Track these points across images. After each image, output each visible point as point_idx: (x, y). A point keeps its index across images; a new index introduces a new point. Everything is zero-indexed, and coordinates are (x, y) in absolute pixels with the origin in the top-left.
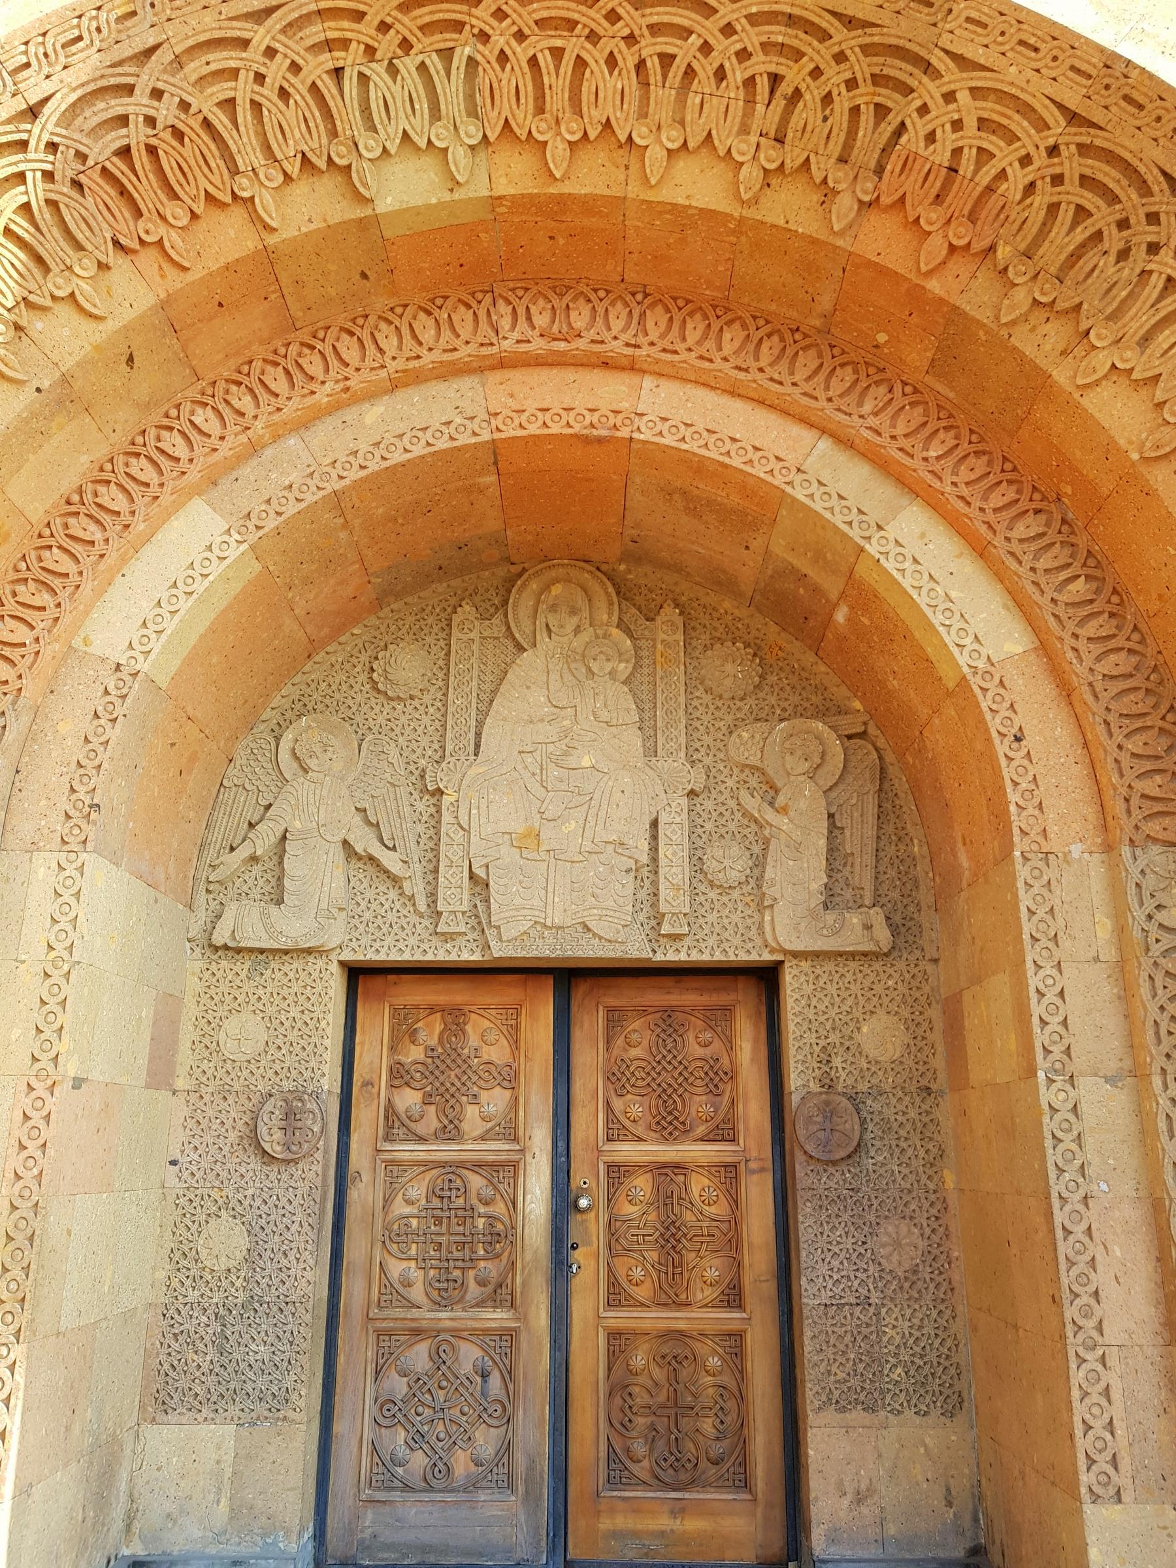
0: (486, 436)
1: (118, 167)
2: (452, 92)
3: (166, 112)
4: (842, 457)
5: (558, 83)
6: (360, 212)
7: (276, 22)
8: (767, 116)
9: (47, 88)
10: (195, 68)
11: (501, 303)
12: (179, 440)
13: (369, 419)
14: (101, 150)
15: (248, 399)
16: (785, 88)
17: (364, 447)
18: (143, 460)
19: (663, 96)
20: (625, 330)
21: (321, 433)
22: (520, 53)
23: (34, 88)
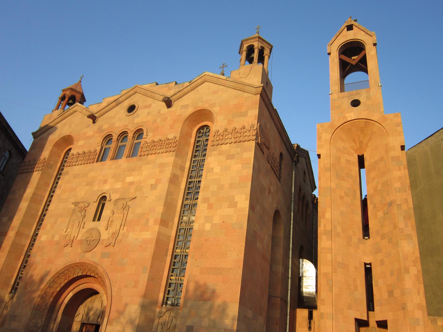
21: (78, 287)
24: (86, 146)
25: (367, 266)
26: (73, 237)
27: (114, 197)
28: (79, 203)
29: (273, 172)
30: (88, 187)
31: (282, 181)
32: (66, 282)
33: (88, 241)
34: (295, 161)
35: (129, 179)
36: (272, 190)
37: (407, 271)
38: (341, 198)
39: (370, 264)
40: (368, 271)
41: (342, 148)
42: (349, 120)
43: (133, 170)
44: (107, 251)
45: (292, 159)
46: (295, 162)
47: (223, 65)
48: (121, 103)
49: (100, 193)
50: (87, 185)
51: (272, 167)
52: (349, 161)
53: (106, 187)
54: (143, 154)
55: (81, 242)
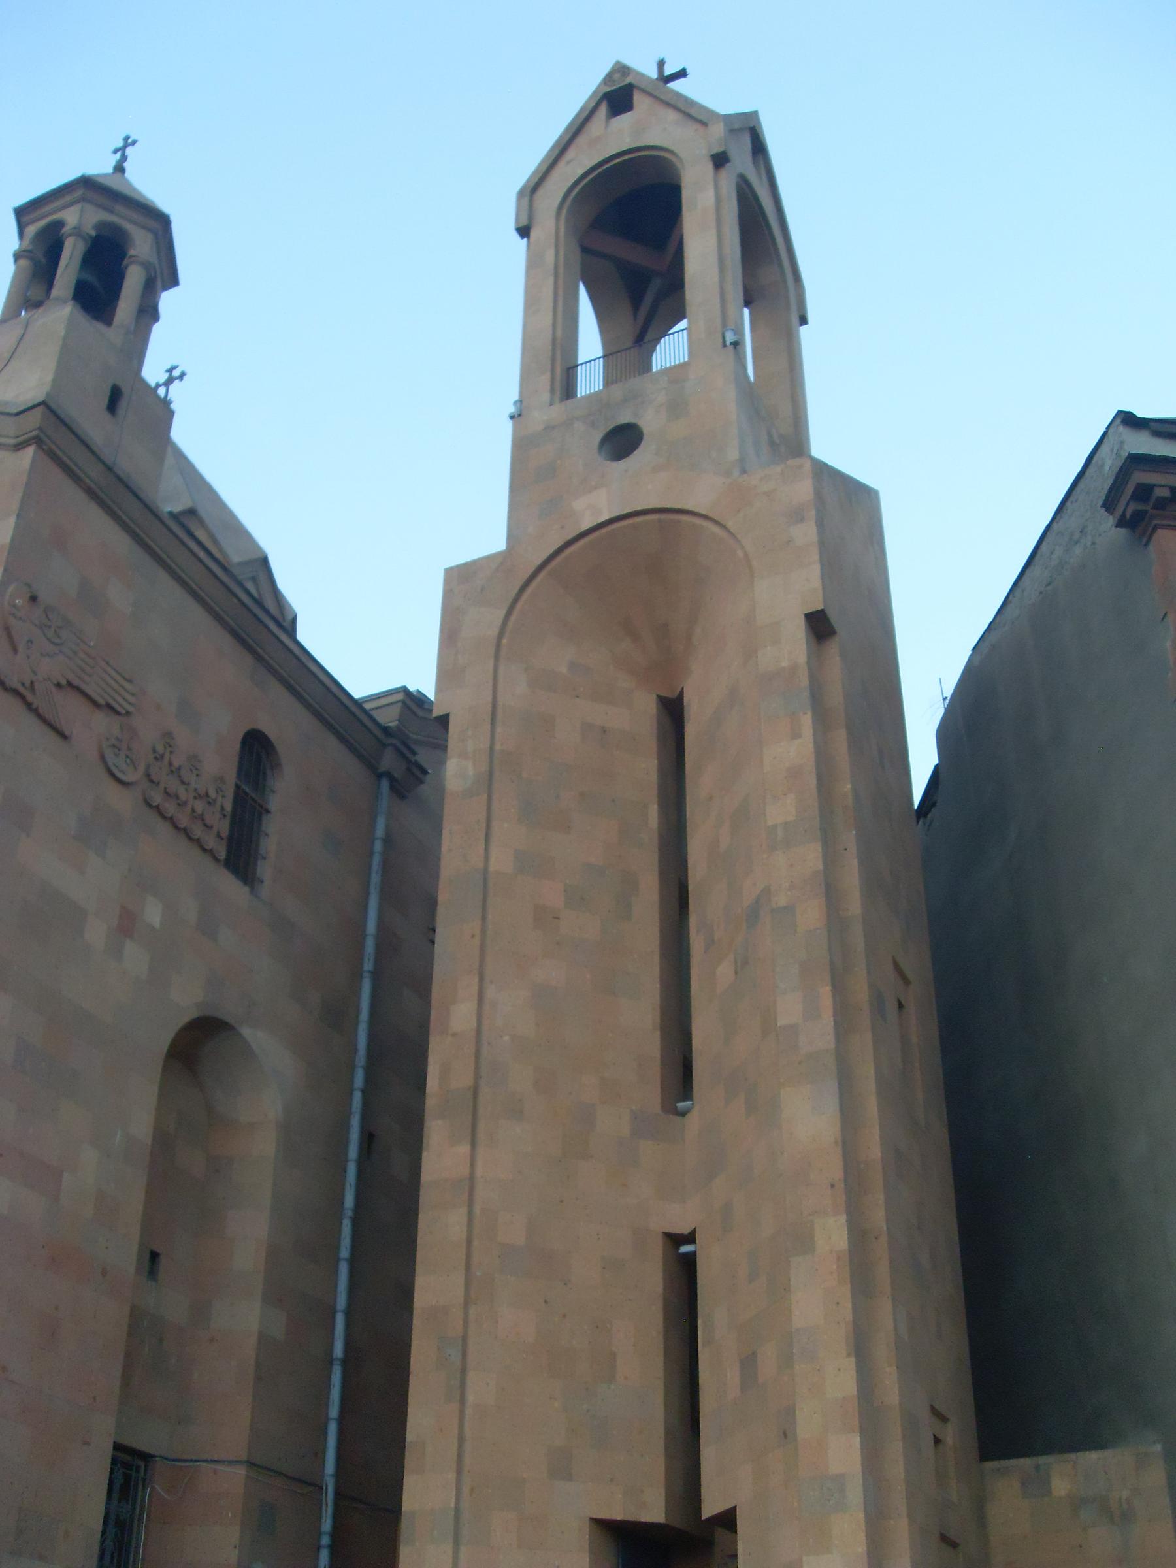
25: (685, 1249)
29: (163, 828)
31: (265, 870)
34: (388, 775)
36: (153, 914)
37: (803, 1241)
38: (544, 917)
39: (691, 1238)
40: (683, 1271)
41: (564, 670)
42: (586, 524)
45: (370, 764)
46: (392, 780)
47: (170, 371)
51: (148, 804)
52: (604, 731)
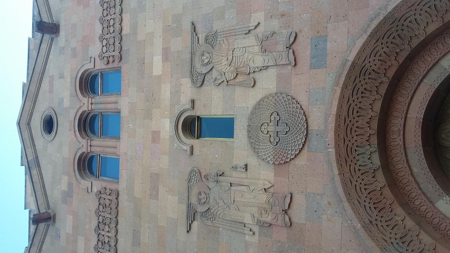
0: (422, 148)
1: (378, 210)
2: (361, 150)
3: (368, 200)
4: (428, 77)
5: (359, 131)
6: (381, 168)
7: (352, 180)
8: (368, 94)
9: (367, 219)
10: (360, 194)
11: (391, 144)
12: (422, 208)
13: (417, 171)
14: (376, 212)
15: (413, 194)
16: (364, 91)
17: (423, 172)
18: (427, 215)
19: (363, 113)
20: (398, 120)
21: (419, 180)
22: (355, 138)
23: (367, 221)
24: (87, 226)
26: (264, 197)
27: (187, 90)
28: (189, 205)
30: (162, 190)
32: (399, 210)
33: (279, 129)
35: (157, 66)
43: (142, 62)
44: (308, 52)
48: (37, 157)
49: (177, 143)
50: (156, 197)
53: (166, 126)
54: (117, 53)
55: (282, 163)
